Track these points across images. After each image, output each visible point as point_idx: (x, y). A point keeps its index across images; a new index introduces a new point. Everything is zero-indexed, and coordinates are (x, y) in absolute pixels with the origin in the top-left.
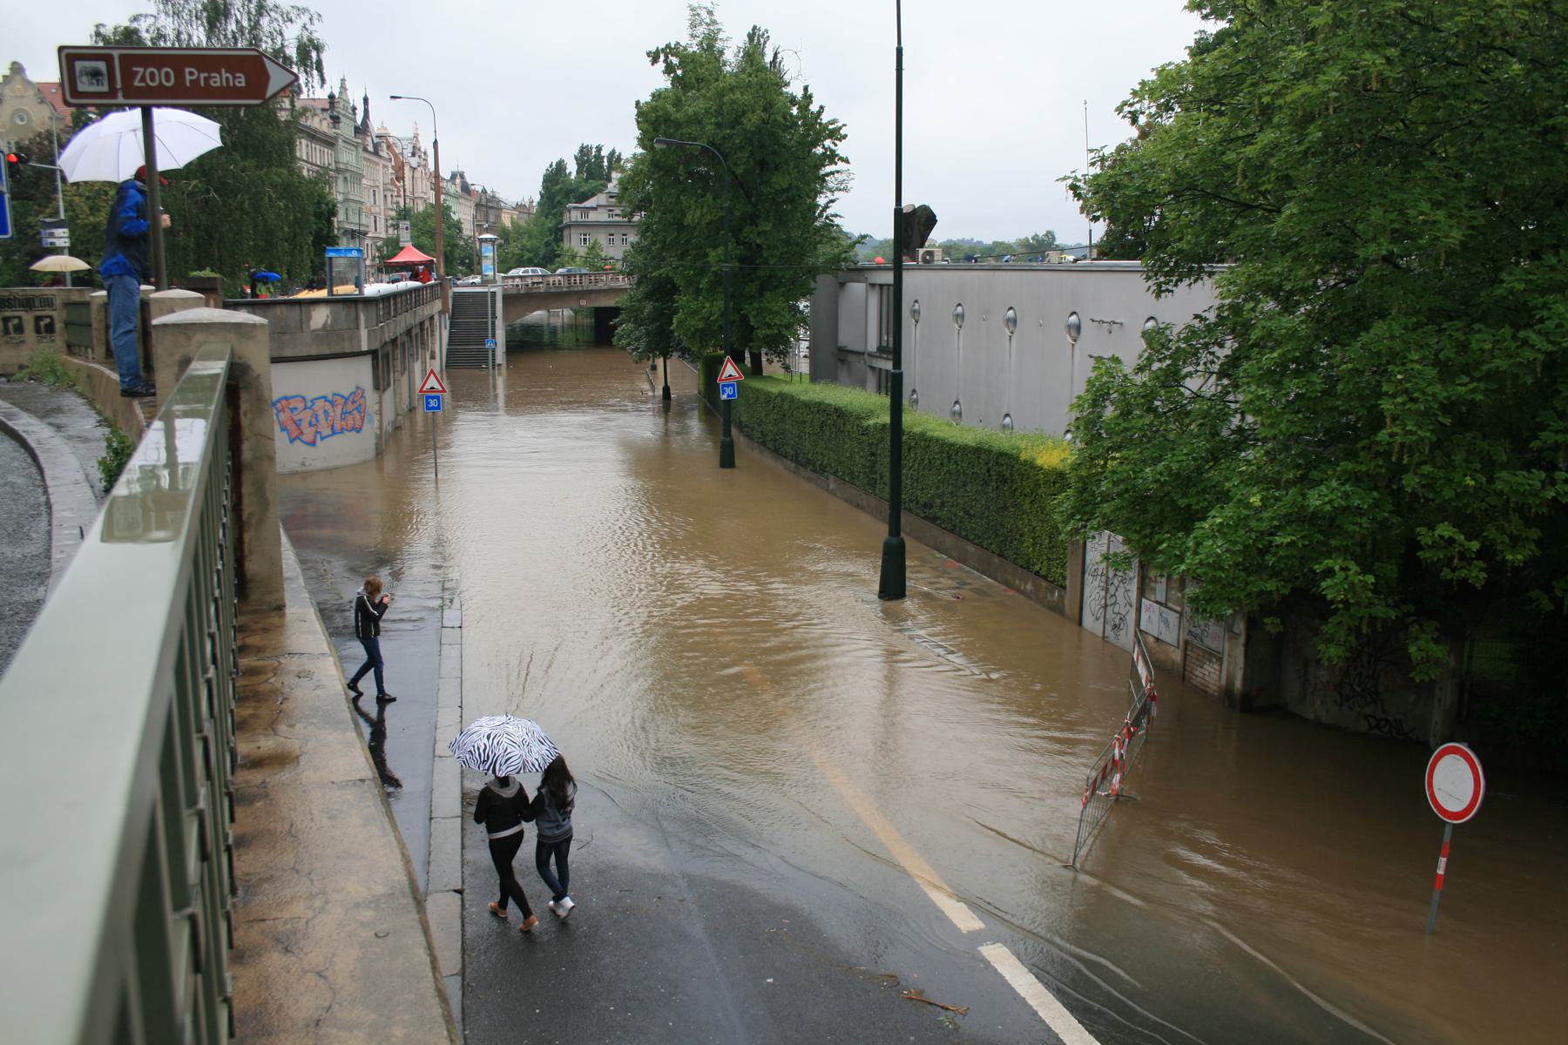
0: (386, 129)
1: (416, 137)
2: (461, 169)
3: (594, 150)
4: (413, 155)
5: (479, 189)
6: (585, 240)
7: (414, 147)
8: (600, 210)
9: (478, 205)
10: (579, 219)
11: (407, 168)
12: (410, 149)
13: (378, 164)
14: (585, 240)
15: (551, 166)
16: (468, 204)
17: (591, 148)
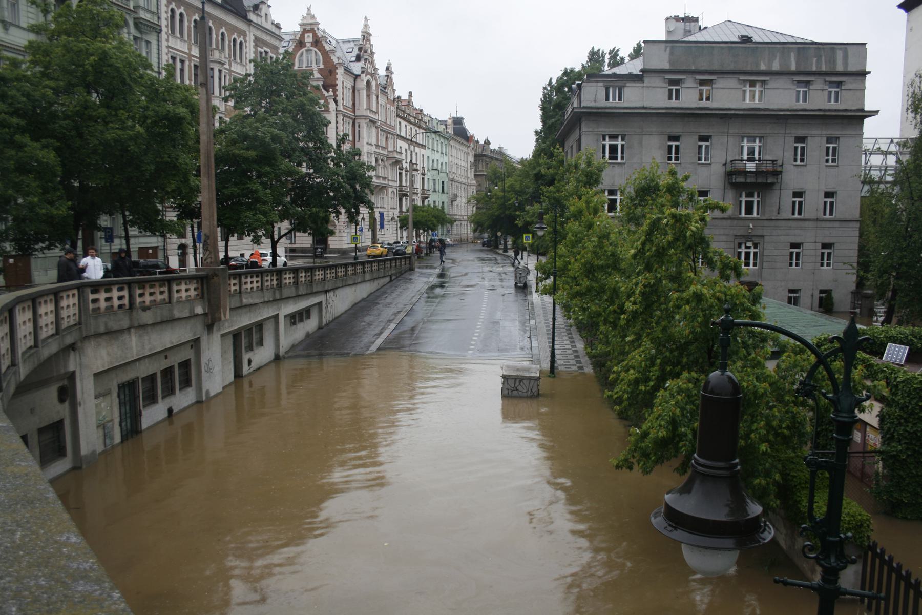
0: (313, 17)
1: (366, 36)
2: (459, 115)
3: (607, 57)
4: (358, 59)
5: (482, 142)
6: (613, 149)
7: (360, 49)
8: (648, 81)
9: (479, 157)
10: (602, 103)
11: (340, 71)
12: (356, 51)
13: (243, 33)
14: (613, 149)
15: (550, 83)
16: (464, 149)
17: (603, 56)
